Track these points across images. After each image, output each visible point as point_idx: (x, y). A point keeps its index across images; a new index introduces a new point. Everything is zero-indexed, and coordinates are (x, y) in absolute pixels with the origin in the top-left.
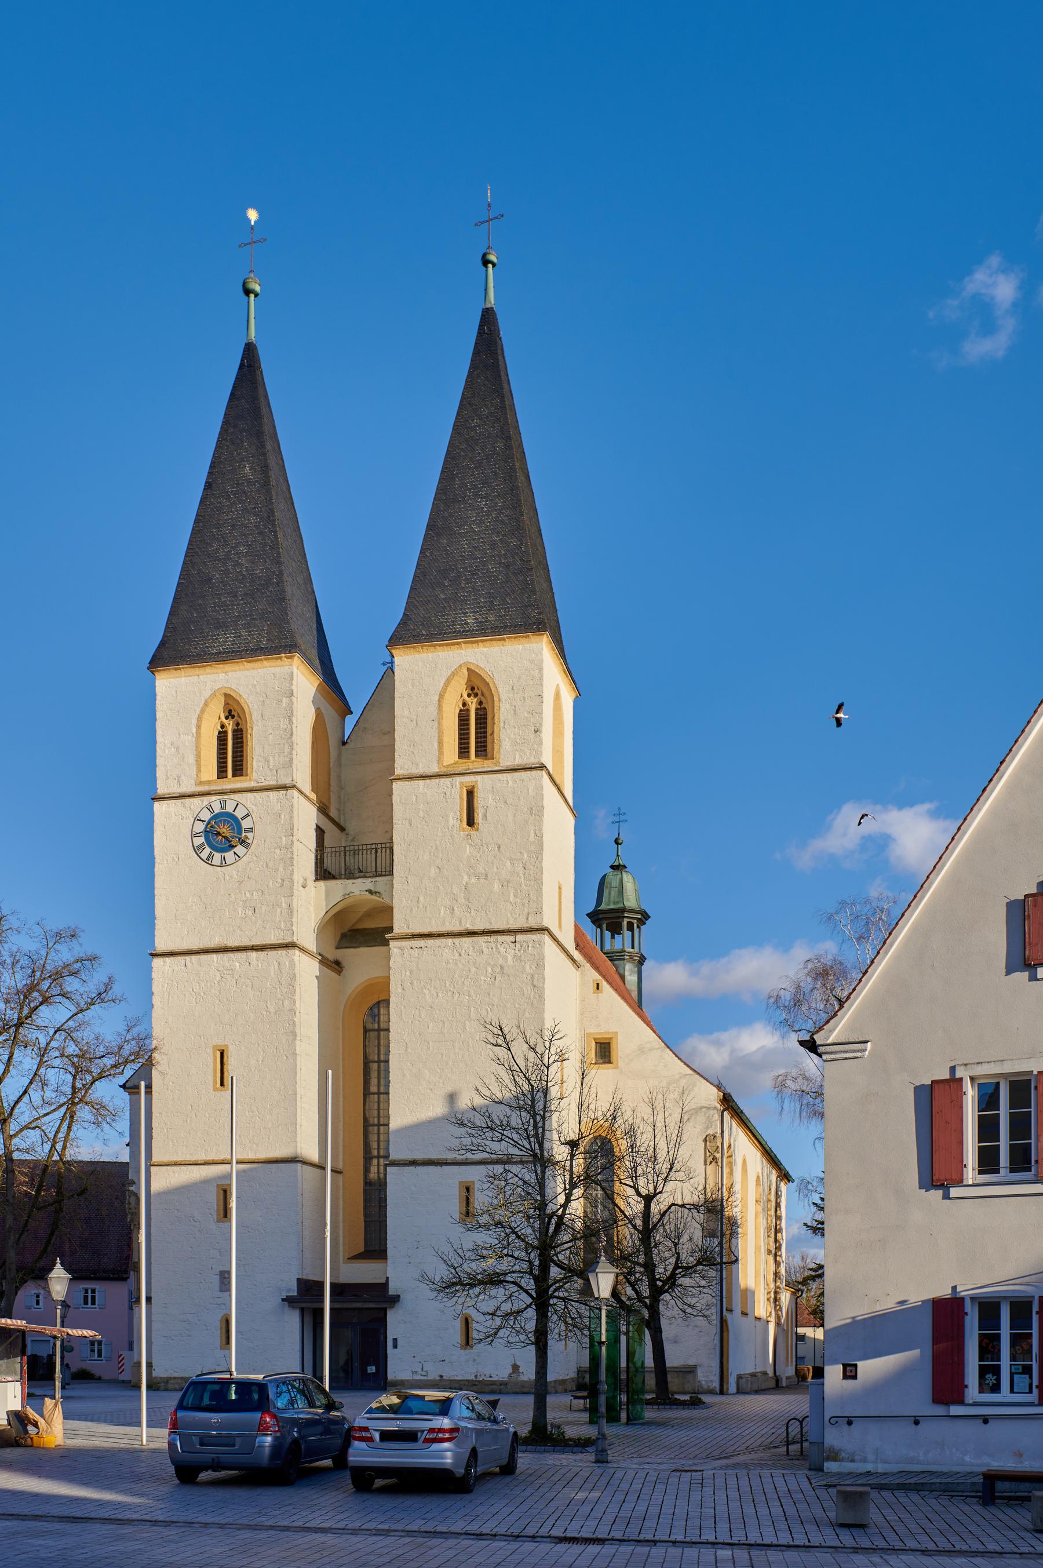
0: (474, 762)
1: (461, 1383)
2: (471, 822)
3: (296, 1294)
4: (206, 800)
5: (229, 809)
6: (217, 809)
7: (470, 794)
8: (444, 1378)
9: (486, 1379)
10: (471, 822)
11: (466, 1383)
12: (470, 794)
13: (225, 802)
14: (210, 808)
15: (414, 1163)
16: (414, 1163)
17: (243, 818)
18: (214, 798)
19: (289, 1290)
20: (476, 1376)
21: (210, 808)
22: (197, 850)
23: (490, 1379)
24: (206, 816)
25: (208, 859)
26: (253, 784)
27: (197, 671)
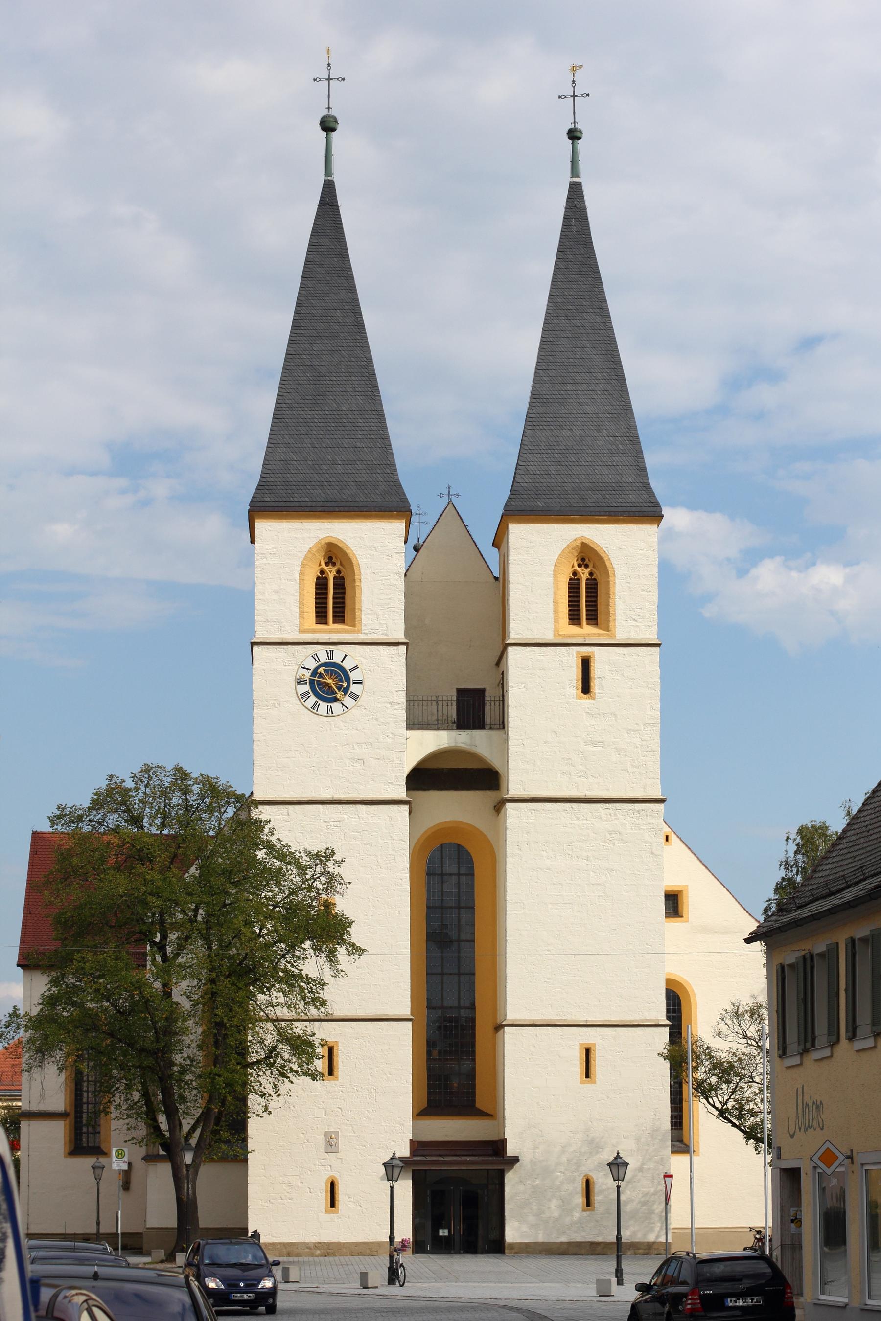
0: (587, 631)
2: (586, 688)
4: (311, 649)
5: (337, 659)
6: (324, 659)
7: (586, 663)
10: (586, 688)
12: (586, 663)
13: (332, 652)
21: (315, 657)
24: (312, 665)
26: (361, 637)
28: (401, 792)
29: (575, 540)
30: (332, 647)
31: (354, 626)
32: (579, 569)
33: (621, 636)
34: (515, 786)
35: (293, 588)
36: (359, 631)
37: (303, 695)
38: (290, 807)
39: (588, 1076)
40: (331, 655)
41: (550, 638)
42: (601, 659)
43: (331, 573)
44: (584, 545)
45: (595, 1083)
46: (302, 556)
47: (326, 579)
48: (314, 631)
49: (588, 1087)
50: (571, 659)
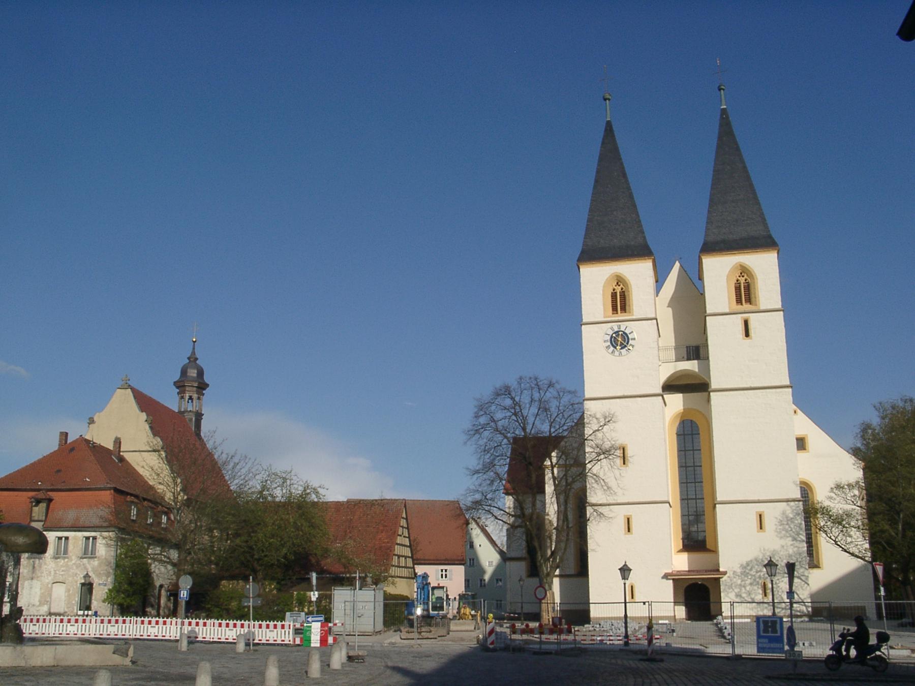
0: (746, 307)
2: (747, 334)
4: (610, 325)
5: (622, 329)
6: (616, 329)
7: (746, 323)
10: (747, 334)
12: (746, 323)
13: (620, 326)
14: (612, 328)
17: (630, 334)
18: (614, 324)
21: (612, 328)
22: (608, 347)
24: (611, 332)
26: (634, 317)
27: (602, 265)
28: (660, 391)
29: (736, 264)
31: (630, 313)
32: (739, 278)
33: (762, 307)
34: (714, 385)
35: (600, 297)
36: (633, 315)
37: (607, 347)
38: (604, 401)
39: (761, 528)
40: (619, 327)
41: (727, 311)
42: (753, 319)
43: (618, 289)
44: (741, 265)
45: (765, 531)
46: (603, 282)
47: (616, 293)
48: (611, 317)
49: (761, 534)
50: (738, 320)
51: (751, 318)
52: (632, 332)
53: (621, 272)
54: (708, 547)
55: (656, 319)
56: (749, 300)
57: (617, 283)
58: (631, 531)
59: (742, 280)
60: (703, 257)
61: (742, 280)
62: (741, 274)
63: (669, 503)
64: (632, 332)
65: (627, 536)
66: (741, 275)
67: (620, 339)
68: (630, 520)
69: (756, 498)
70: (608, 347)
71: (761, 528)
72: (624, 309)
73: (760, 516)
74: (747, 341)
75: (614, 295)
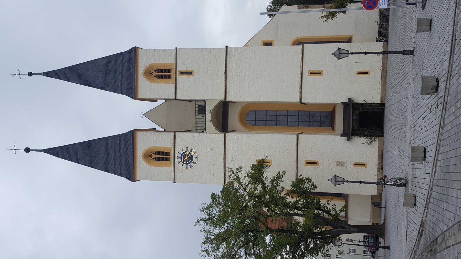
1: (383, 75)
2: (190, 73)
3: (346, 137)
7: (182, 73)
8: (380, 81)
9: (382, 66)
10: (190, 73)
11: (383, 73)
12: (182, 73)
13: (177, 157)
15: (301, 92)
16: (301, 92)
19: (345, 140)
20: (380, 69)
21: (179, 162)
23: (382, 64)
25: (195, 164)
30: (176, 157)
39: (320, 73)
40: (178, 157)
41: (174, 85)
42: (181, 68)
45: (323, 70)
48: (171, 162)
50: (181, 78)
51: (180, 69)
52: (182, 149)
53: (142, 153)
54: (331, 110)
55: (175, 132)
56: (169, 70)
57: (150, 156)
58: (316, 162)
59: (155, 74)
60: (137, 98)
61: (155, 74)
62: (151, 73)
63: (298, 134)
64: (182, 149)
65: (319, 165)
66: (151, 74)
67: (186, 158)
68: (308, 162)
69: (300, 76)
70: (191, 166)
71: (320, 73)
72: (168, 154)
73: (311, 73)
74: (194, 73)
75: (158, 159)
